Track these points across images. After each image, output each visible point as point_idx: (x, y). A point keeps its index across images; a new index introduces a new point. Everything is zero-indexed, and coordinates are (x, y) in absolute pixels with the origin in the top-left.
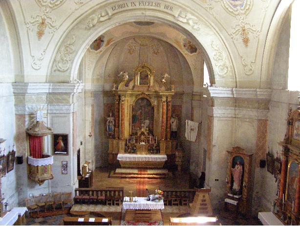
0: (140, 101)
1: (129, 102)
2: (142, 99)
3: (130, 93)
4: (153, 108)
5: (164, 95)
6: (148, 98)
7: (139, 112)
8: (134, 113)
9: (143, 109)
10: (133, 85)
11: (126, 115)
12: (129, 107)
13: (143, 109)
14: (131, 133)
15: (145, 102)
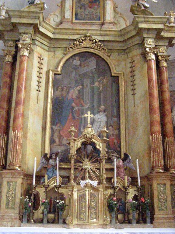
0: (77, 62)
1: (45, 61)
2: (84, 55)
3: (50, 35)
4: (116, 79)
5: (149, 29)
6: (101, 54)
7: (74, 93)
8: (58, 93)
9: (87, 81)
10: (58, 20)
11: (33, 94)
12: (44, 76)
13: (87, 81)
14: (47, 151)
15: (92, 64)
